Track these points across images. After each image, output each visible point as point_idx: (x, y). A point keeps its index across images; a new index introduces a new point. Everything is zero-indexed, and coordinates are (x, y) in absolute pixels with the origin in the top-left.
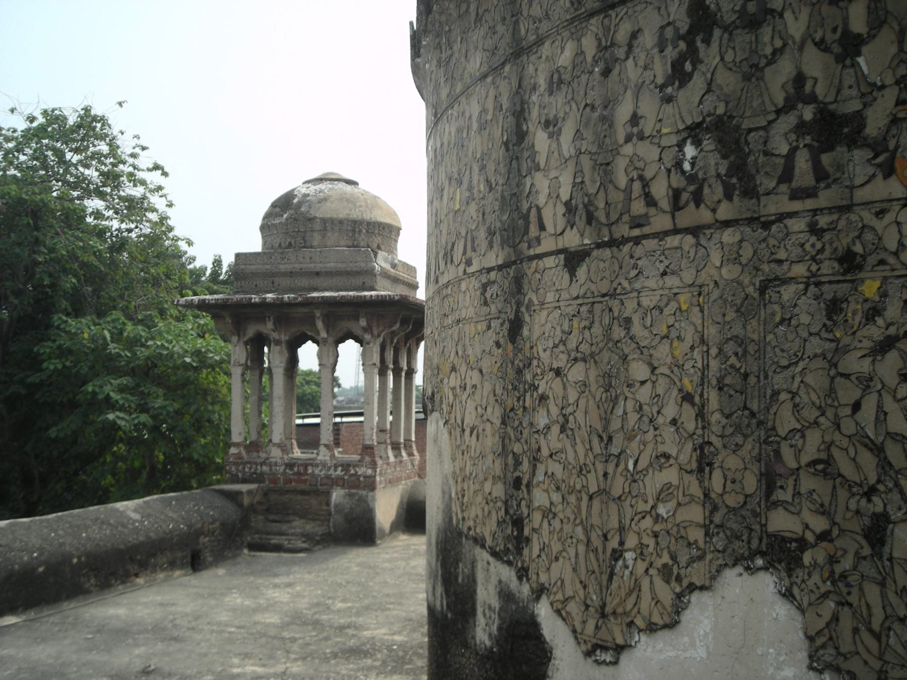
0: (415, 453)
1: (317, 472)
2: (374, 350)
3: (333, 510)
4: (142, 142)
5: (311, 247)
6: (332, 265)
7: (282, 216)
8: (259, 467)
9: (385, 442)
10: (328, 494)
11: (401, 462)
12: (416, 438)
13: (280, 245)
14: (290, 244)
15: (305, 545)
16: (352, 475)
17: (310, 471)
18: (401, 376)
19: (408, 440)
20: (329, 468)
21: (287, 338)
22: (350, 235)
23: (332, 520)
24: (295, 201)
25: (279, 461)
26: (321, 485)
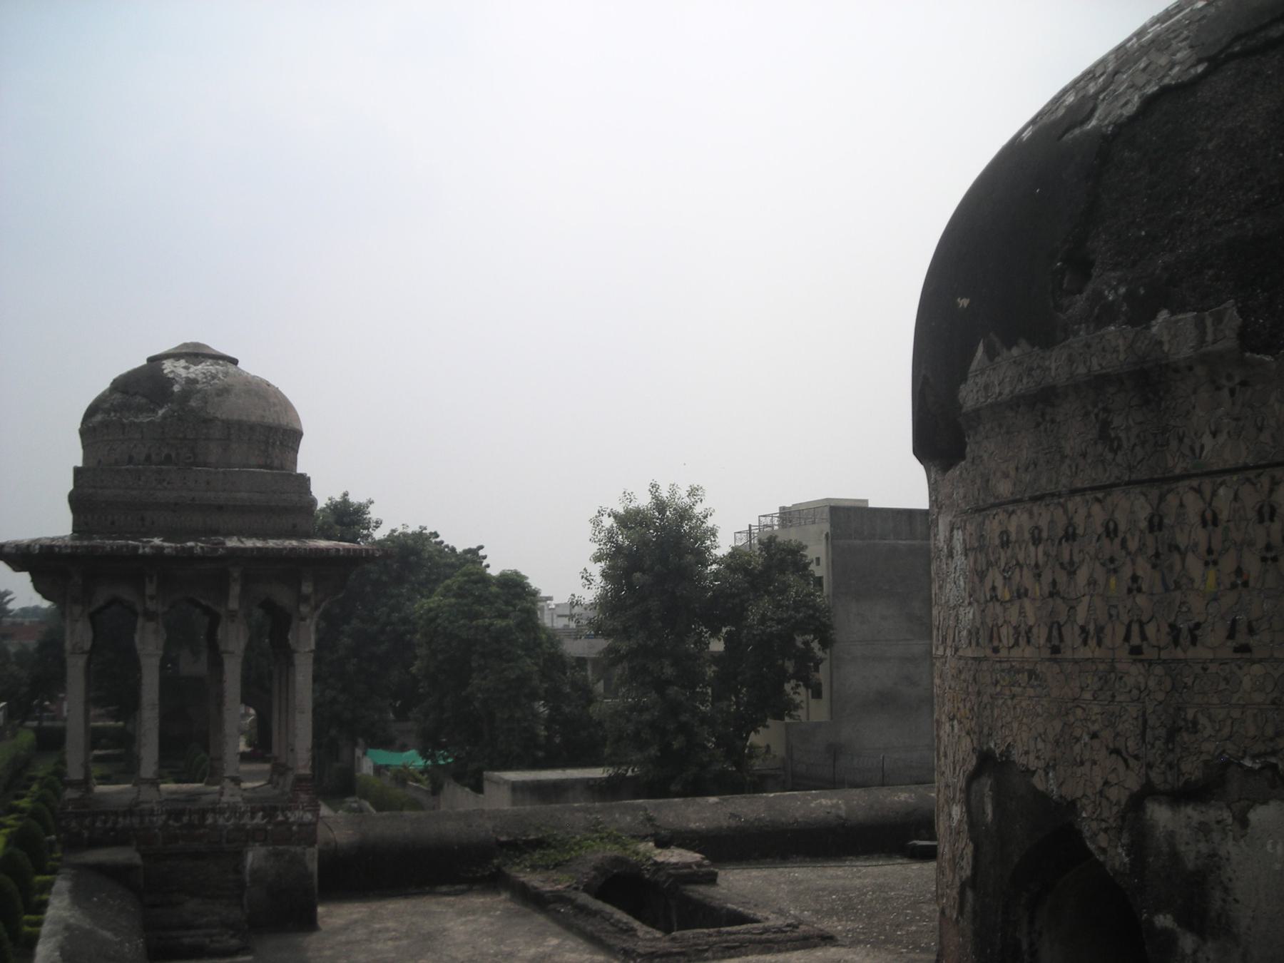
1: (221, 821)
3: (248, 879)
7: (154, 411)
8: (120, 819)
10: (240, 855)
13: (148, 458)
14: (168, 457)
15: (234, 942)
16: (281, 823)
17: (210, 821)
24: (176, 388)
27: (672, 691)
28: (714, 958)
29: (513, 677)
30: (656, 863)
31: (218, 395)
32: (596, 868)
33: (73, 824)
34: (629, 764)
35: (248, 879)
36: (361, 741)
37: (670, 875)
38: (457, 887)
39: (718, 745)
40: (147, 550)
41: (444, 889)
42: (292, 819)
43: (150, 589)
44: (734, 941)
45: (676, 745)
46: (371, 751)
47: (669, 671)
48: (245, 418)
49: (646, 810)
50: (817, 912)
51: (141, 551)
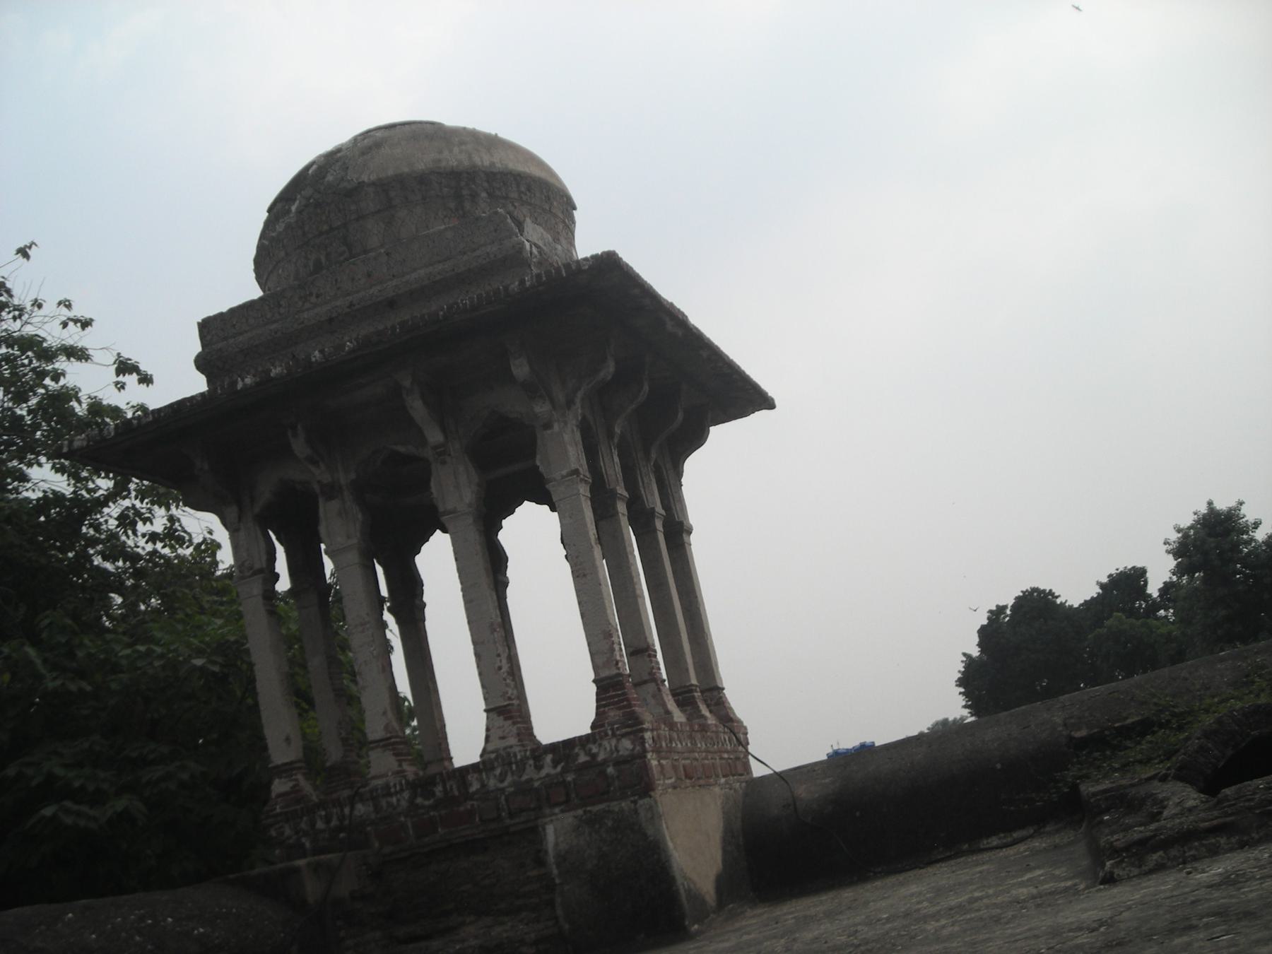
1: (492, 783)
2: (567, 437)
3: (555, 872)
4: (76, 312)
5: (366, 252)
6: (422, 272)
7: (289, 211)
10: (534, 833)
14: (318, 267)
16: (586, 766)
17: (475, 787)
18: (655, 530)
20: (522, 765)
21: (353, 476)
22: (452, 205)
23: (558, 900)
25: (392, 780)
26: (511, 815)
31: (363, 154)
33: (288, 831)
35: (555, 872)
38: (1015, 835)
40: (248, 380)
41: (995, 841)
42: (601, 757)
43: (299, 446)
48: (406, 170)
51: (240, 386)
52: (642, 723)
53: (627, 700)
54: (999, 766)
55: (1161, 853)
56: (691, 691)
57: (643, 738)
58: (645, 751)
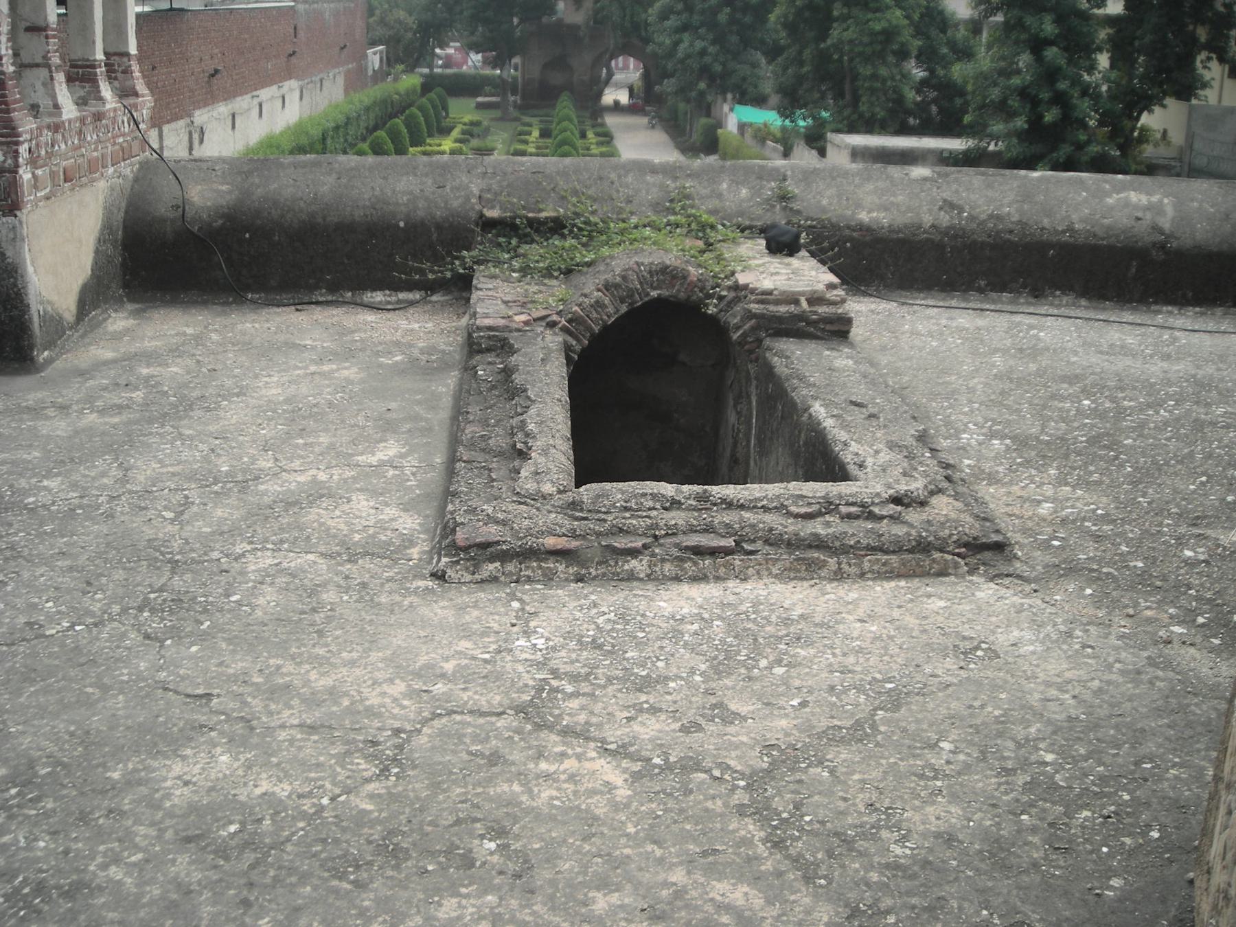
0: (141, 87)
9: (48, 66)
11: (98, 117)
12: (139, 47)
19: (116, 56)
27: (1051, 53)
28: (650, 577)
29: (878, 28)
30: (737, 287)
32: (608, 287)
34: (992, 137)
36: (729, 96)
37: (750, 315)
38: (402, 295)
39: (1101, 123)
41: (378, 297)
44: (729, 530)
45: (1048, 118)
46: (738, 108)
47: (1049, 27)
49: (785, 180)
50: (1022, 442)
52: (19, 135)
53: (6, 104)
54: (402, 224)
55: (498, 564)
56: (94, 67)
57: (16, 152)
58: (17, 166)
